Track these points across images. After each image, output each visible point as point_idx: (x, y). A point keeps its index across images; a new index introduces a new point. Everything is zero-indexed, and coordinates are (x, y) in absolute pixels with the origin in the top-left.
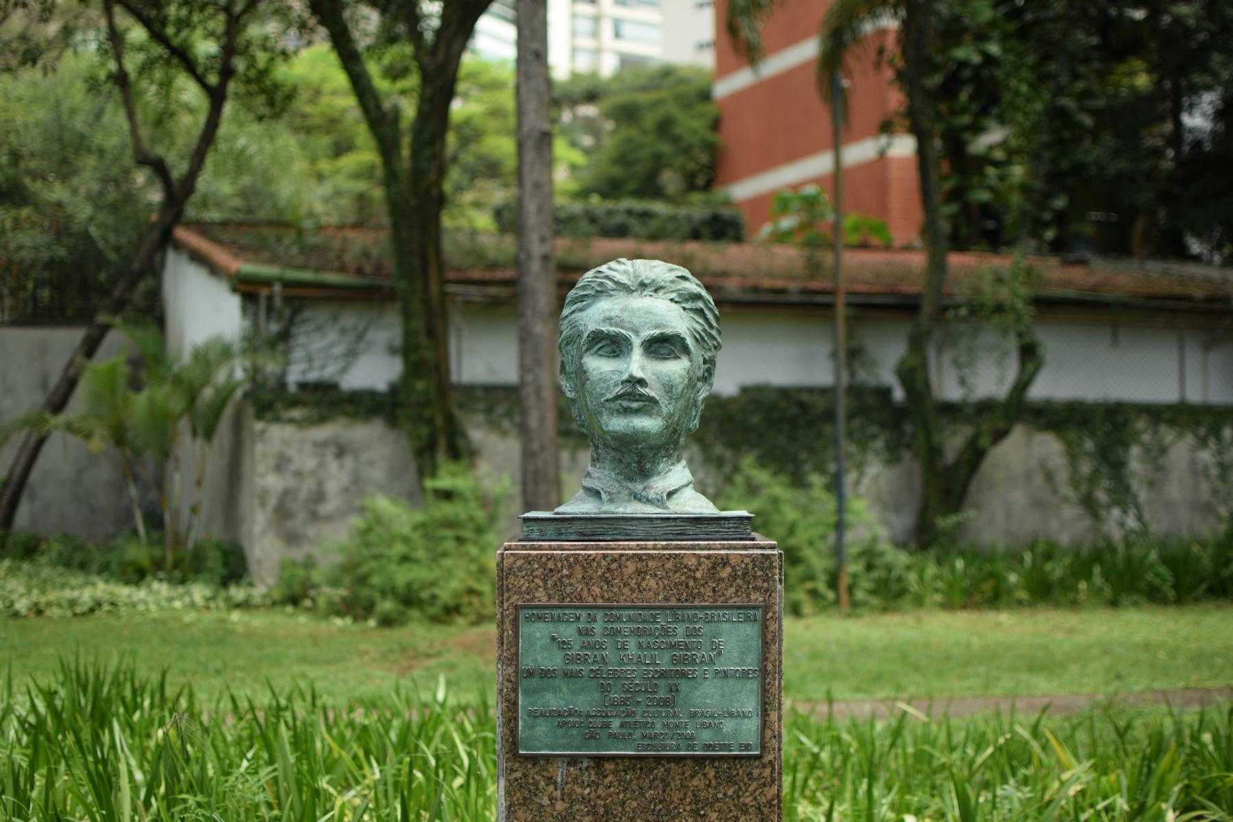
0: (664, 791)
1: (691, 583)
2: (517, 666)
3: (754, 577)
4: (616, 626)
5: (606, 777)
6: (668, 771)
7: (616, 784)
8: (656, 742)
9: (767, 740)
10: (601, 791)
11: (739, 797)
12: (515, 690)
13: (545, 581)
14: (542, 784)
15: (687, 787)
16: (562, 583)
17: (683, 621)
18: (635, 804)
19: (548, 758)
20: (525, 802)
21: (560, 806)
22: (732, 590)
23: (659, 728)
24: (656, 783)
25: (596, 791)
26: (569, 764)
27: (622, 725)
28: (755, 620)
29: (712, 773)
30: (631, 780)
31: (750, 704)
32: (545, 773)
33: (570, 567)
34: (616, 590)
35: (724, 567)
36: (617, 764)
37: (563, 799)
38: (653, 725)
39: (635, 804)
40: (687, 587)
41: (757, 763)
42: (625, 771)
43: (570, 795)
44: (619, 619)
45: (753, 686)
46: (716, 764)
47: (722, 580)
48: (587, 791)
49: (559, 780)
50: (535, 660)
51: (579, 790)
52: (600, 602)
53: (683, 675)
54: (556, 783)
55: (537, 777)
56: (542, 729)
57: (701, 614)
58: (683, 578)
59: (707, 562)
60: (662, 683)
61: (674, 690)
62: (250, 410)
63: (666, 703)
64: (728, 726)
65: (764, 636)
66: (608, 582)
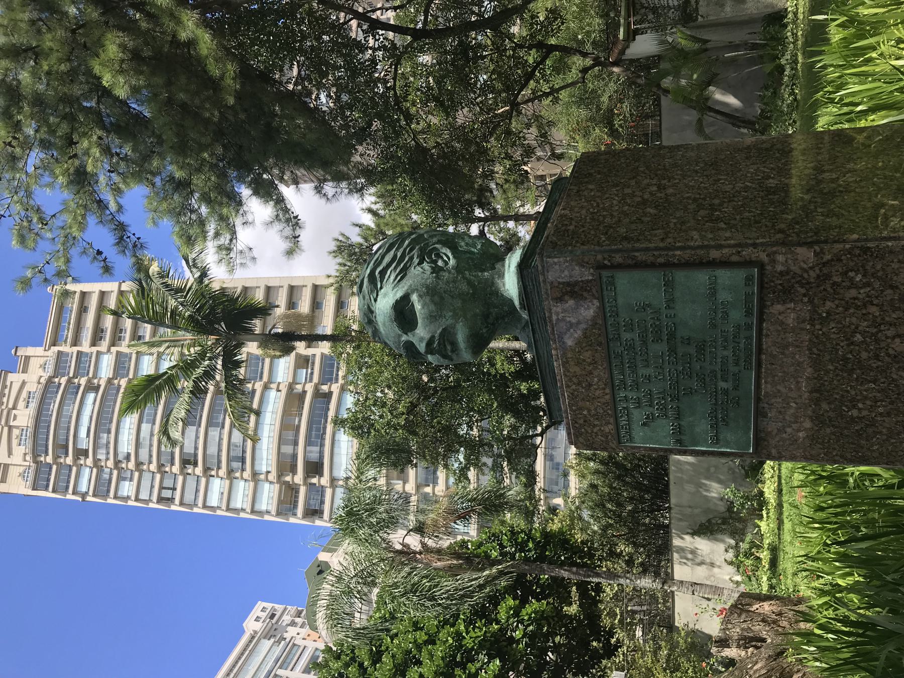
4: (629, 383)
5: (779, 391)
9: (742, 260)
11: (808, 283)
13: (595, 426)
16: (594, 415)
23: (728, 353)
31: (702, 277)
33: (581, 409)
37: (801, 423)
41: (769, 268)
42: (774, 376)
44: (623, 382)
45: (680, 276)
53: (672, 336)
57: (610, 321)
60: (681, 350)
61: (688, 341)
62: (692, 24)
63: (701, 348)
64: (724, 296)
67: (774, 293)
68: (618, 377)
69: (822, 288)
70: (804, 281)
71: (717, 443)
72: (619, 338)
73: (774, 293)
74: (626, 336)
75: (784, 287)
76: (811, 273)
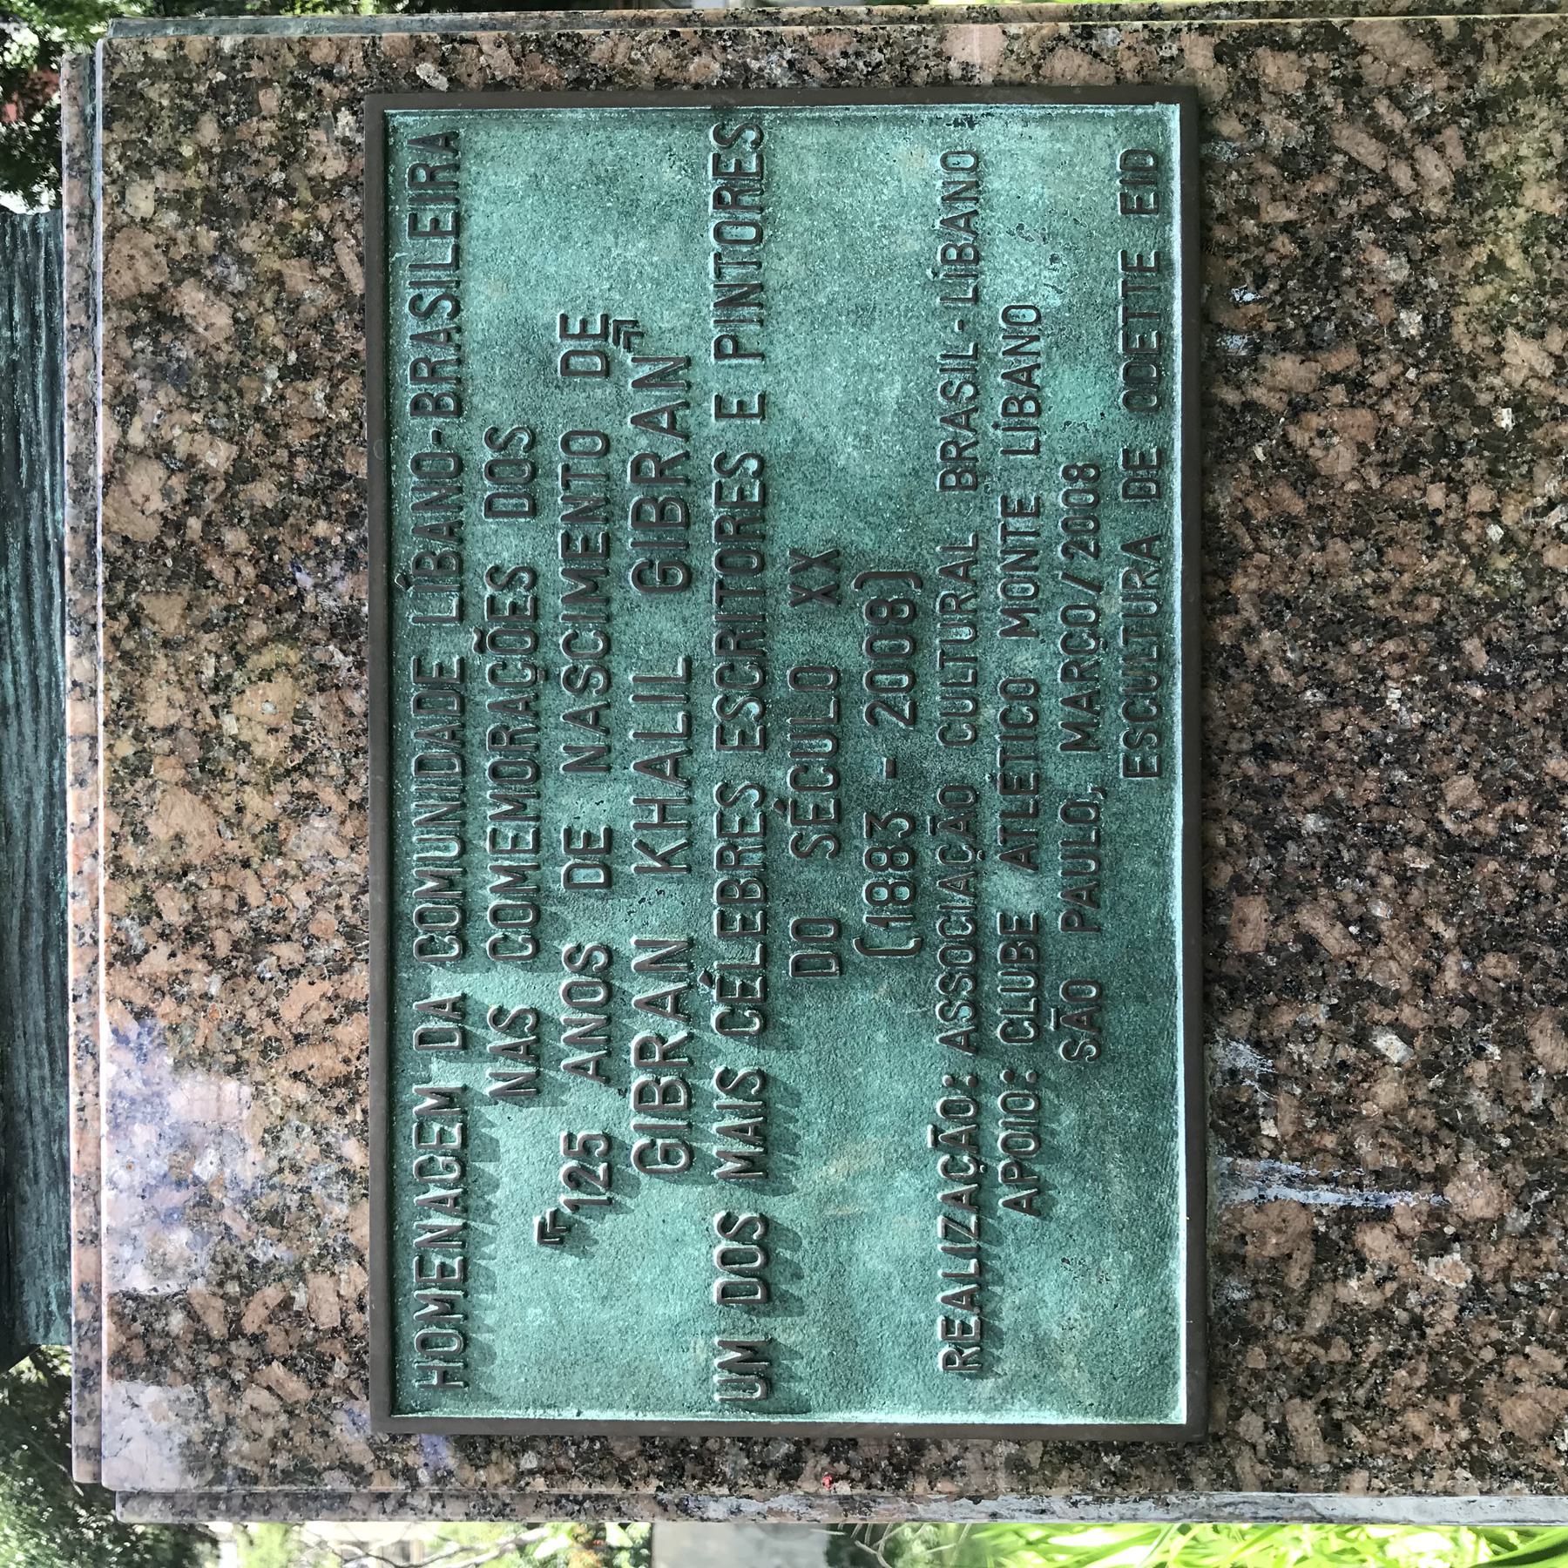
0: (1388, 629)
1: (263, 493)
2: (706, 1432)
3: (231, 156)
4: (489, 892)
5: (1310, 943)
6: (1274, 608)
7: (1349, 888)
8: (1114, 671)
9: (1102, 74)
10: (1392, 969)
11: (1419, 222)
12: (841, 1444)
14: (1354, 1289)
15: (1366, 501)
17: (454, 532)
18: (1460, 787)
19: (1210, 1263)
20: (1459, 1381)
21: (1474, 1196)
22: (297, 275)
24: (1342, 670)
25: (1391, 999)
26: (1245, 1145)
27: (1024, 857)
28: (449, 140)
29: (1289, 369)
30: (1329, 807)
31: (904, 159)
32: (1296, 1276)
34: (299, 894)
35: (179, 325)
36: (1240, 885)
37: (1439, 1179)
38: (1027, 691)
39: (1460, 787)
40: (278, 516)
41: (1229, 126)
43: (1411, 1139)
45: (803, 148)
46: (1236, 344)
47: (244, 328)
48: (1390, 1045)
49: (1329, 1198)
50: (676, 1331)
51: (1387, 1092)
52: (361, 981)
53: (746, 530)
54: (1346, 1216)
55: (1318, 1319)
56: (1049, 1292)
57: (417, 434)
58: (235, 538)
59: (149, 411)
60: (791, 645)
61: (825, 577)
64: (1020, 276)
65: (547, 96)
66: (261, 939)
67: (1260, 281)
68: (428, 849)
69: (1480, 254)
70: (1397, 213)
71: (981, 1367)
72: (454, 567)
73: (1260, 281)
74: (499, 543)
75: (1303, 243)
76: (1429, 161)
